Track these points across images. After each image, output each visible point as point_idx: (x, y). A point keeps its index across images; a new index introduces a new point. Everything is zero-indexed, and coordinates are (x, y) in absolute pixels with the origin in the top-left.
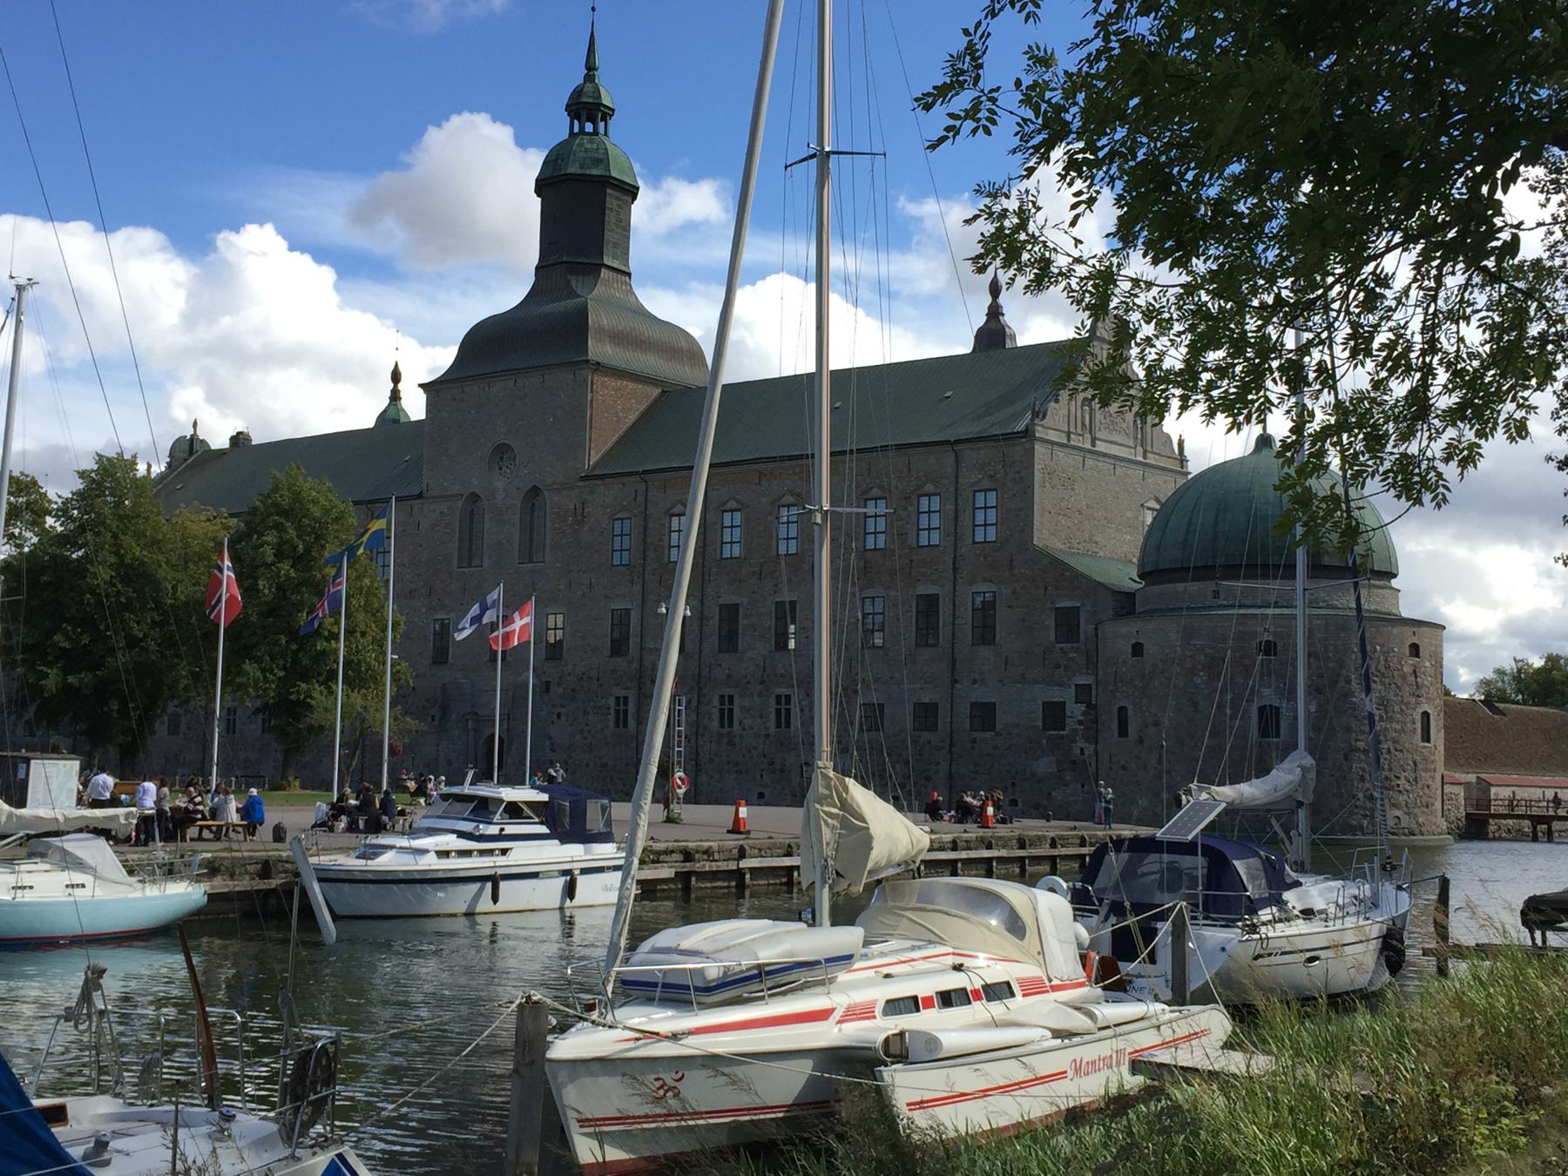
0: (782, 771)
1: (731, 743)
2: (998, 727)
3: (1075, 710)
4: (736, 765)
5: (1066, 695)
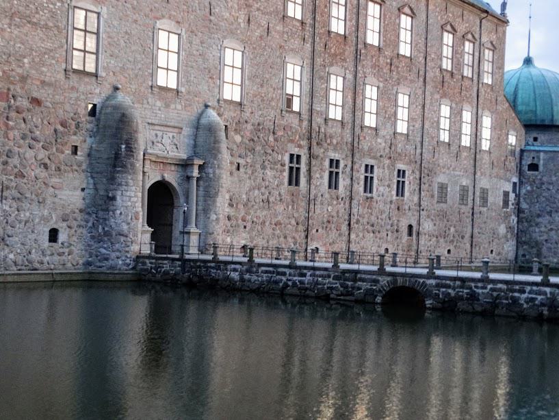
2: (489, 204)
4: (373, 226)
5: (509, 188)
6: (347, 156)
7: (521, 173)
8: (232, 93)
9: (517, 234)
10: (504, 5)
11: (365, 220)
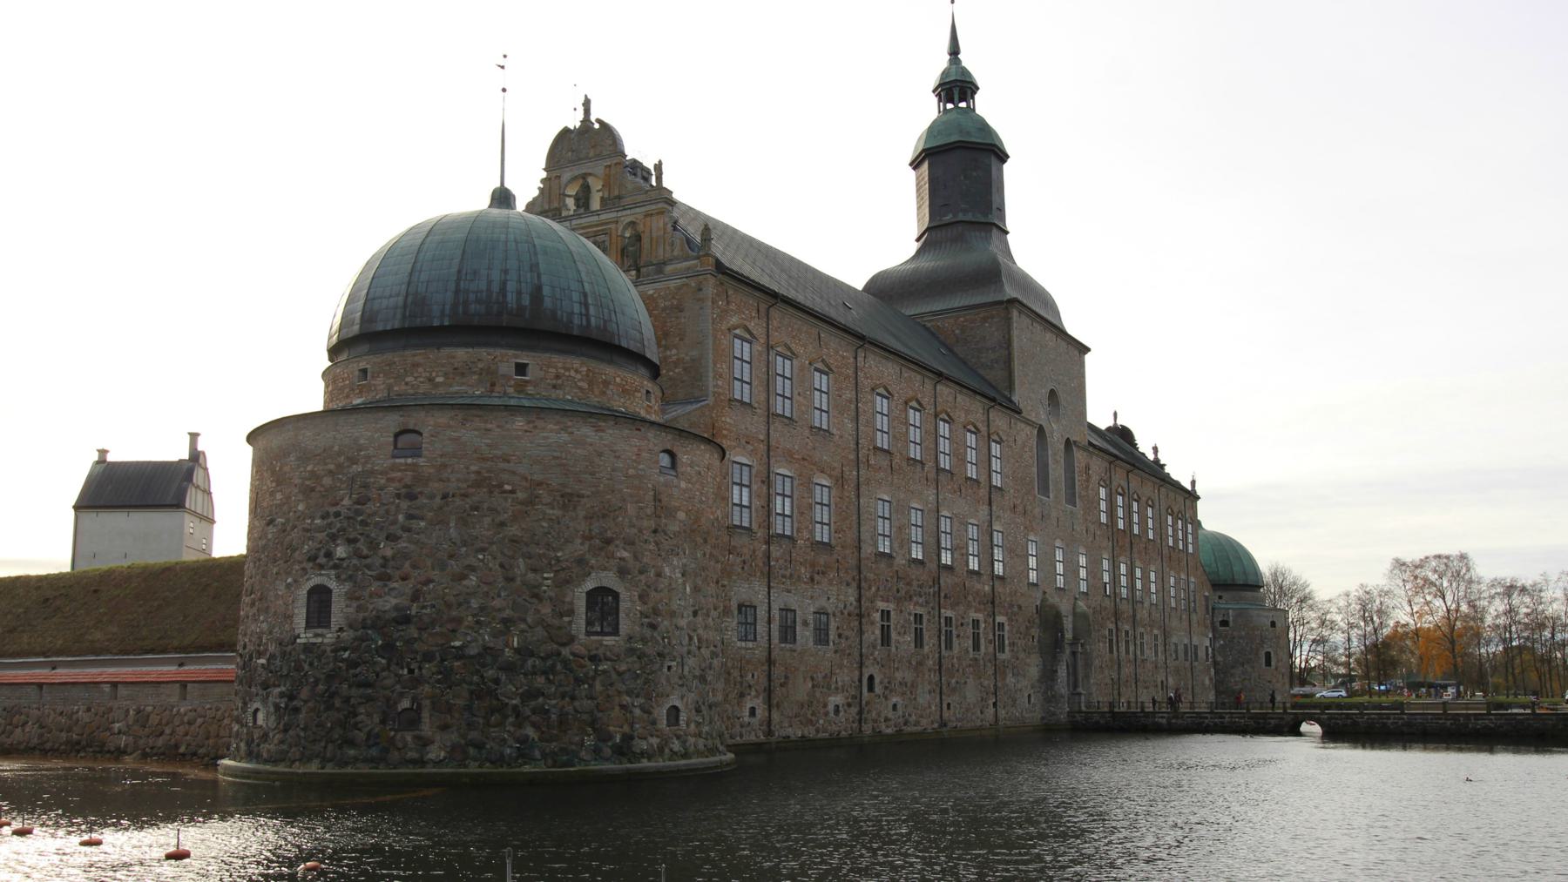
7: (1214, 630)
8: (1083, 587)
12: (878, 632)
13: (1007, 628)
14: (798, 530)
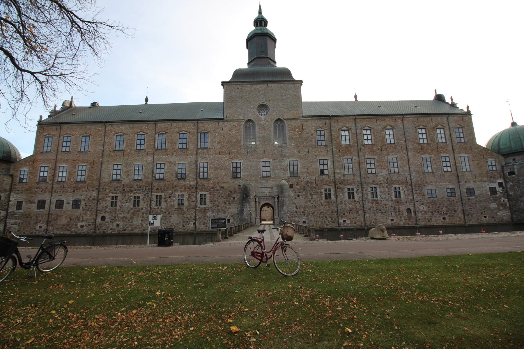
0: (399, 211)
1: (377, 203)
3: (499, 190)
4: (380, 210)
5: (496, 185)
6: (358, 186)
7: (504, 178)
9: (510, 207)
10: (468, 107)
11: (375, 208)
12: (109, 203)
13: (208, 195)
14: (68, 179)
